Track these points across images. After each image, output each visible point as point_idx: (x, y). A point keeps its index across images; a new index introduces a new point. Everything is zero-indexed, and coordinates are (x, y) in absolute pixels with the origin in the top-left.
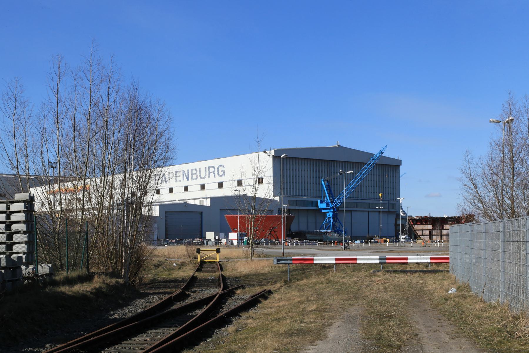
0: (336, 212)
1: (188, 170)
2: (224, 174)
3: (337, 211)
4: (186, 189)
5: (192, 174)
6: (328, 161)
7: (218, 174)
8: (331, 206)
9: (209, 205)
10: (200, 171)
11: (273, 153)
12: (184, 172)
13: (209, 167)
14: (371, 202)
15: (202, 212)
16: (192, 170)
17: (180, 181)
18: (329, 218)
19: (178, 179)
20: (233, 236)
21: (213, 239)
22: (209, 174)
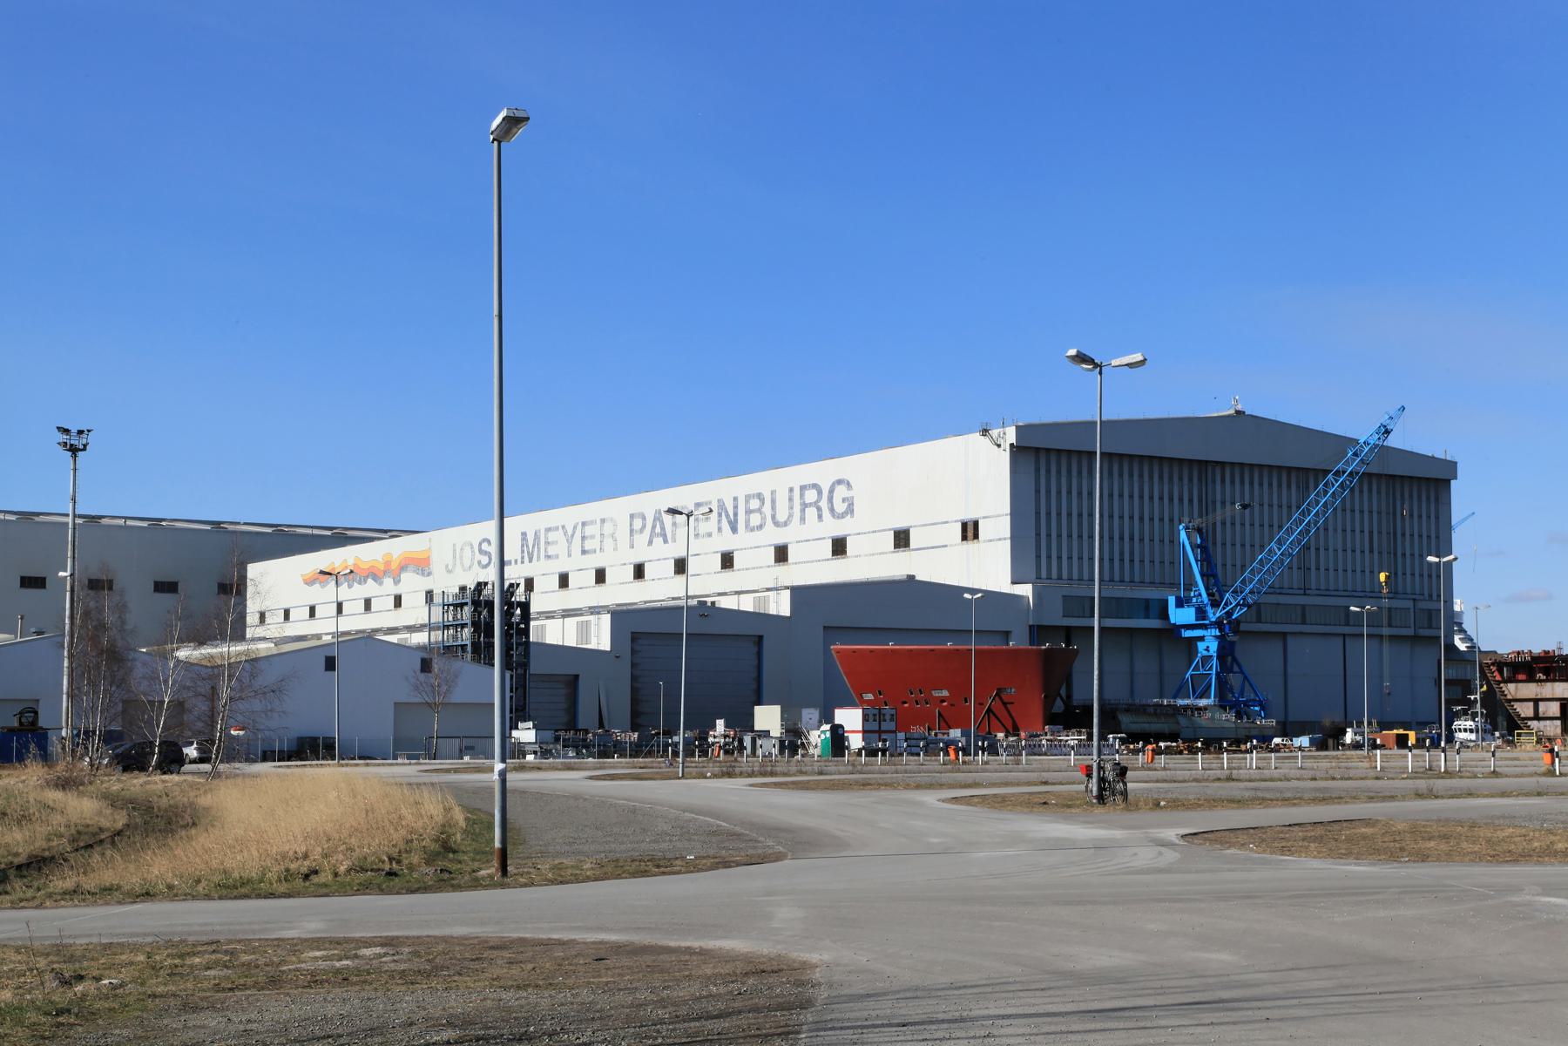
0: (1231, 637)
1: (735, 499)
2: (850, 510)
3: (1230, 633)
4: (727, 561)
5: (749, 512)
6: (1203, 464)
7: (832, 510)
8: (1213, 615)
9: (788, 614)
10: (773, 502)
11: (1011, 436)
13: (803, 488)
15: (761, 638)
16: (748, 498)
17: (710, 535)
18: (1206, 659)
20: (850, 719)
21: (776, 731)
22: (803, 511)
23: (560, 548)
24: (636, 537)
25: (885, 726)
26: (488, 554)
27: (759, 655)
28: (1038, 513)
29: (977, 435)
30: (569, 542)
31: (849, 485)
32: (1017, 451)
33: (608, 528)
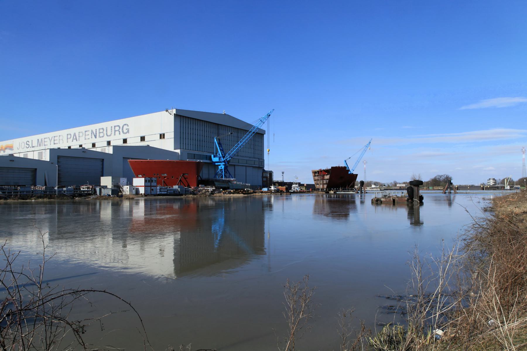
0: (227, 165)
2: (128, 132)
3: (227, 164)
5: (100, 133)
6: (218, 125)
7: (123, 132)
8: (222, 159)
10: (107, 130)
11: (174, 111)
12: (92, 132)
13: (115, 127)
14: (248, 159)
15: (103, 160)
16: (100, 129)
19: (87, 137)
21: (110, 186)
22: (115, 132)
23: (48, 143)
24: (69, 140)
25: (153, 184)
26: (29, 145)
27: (103, 164)
28: (181, 132)
29: (165, 112)
30: (50, 141)
31: (128, 125)
32: (176, 116)
33: (61, 138)
